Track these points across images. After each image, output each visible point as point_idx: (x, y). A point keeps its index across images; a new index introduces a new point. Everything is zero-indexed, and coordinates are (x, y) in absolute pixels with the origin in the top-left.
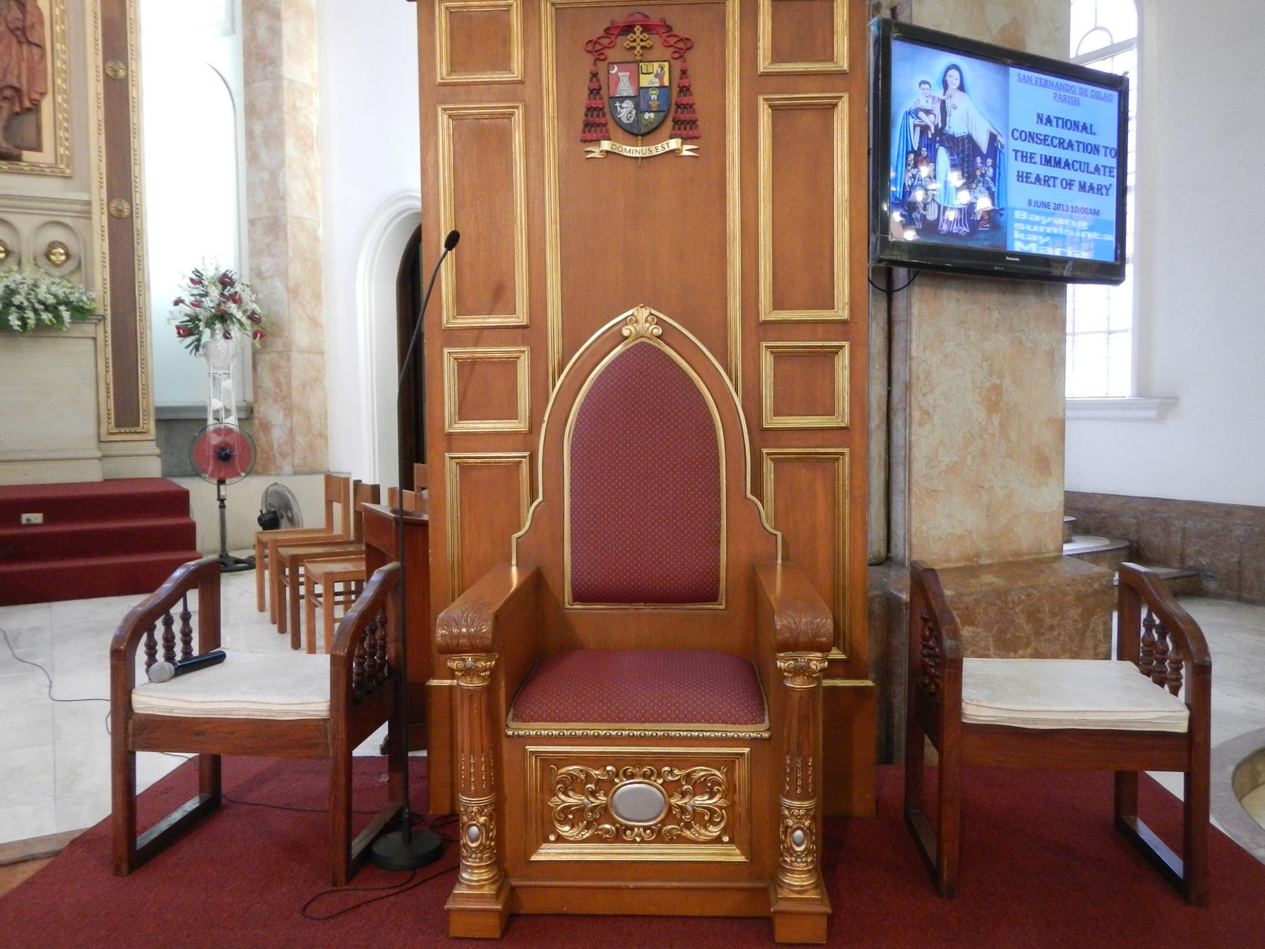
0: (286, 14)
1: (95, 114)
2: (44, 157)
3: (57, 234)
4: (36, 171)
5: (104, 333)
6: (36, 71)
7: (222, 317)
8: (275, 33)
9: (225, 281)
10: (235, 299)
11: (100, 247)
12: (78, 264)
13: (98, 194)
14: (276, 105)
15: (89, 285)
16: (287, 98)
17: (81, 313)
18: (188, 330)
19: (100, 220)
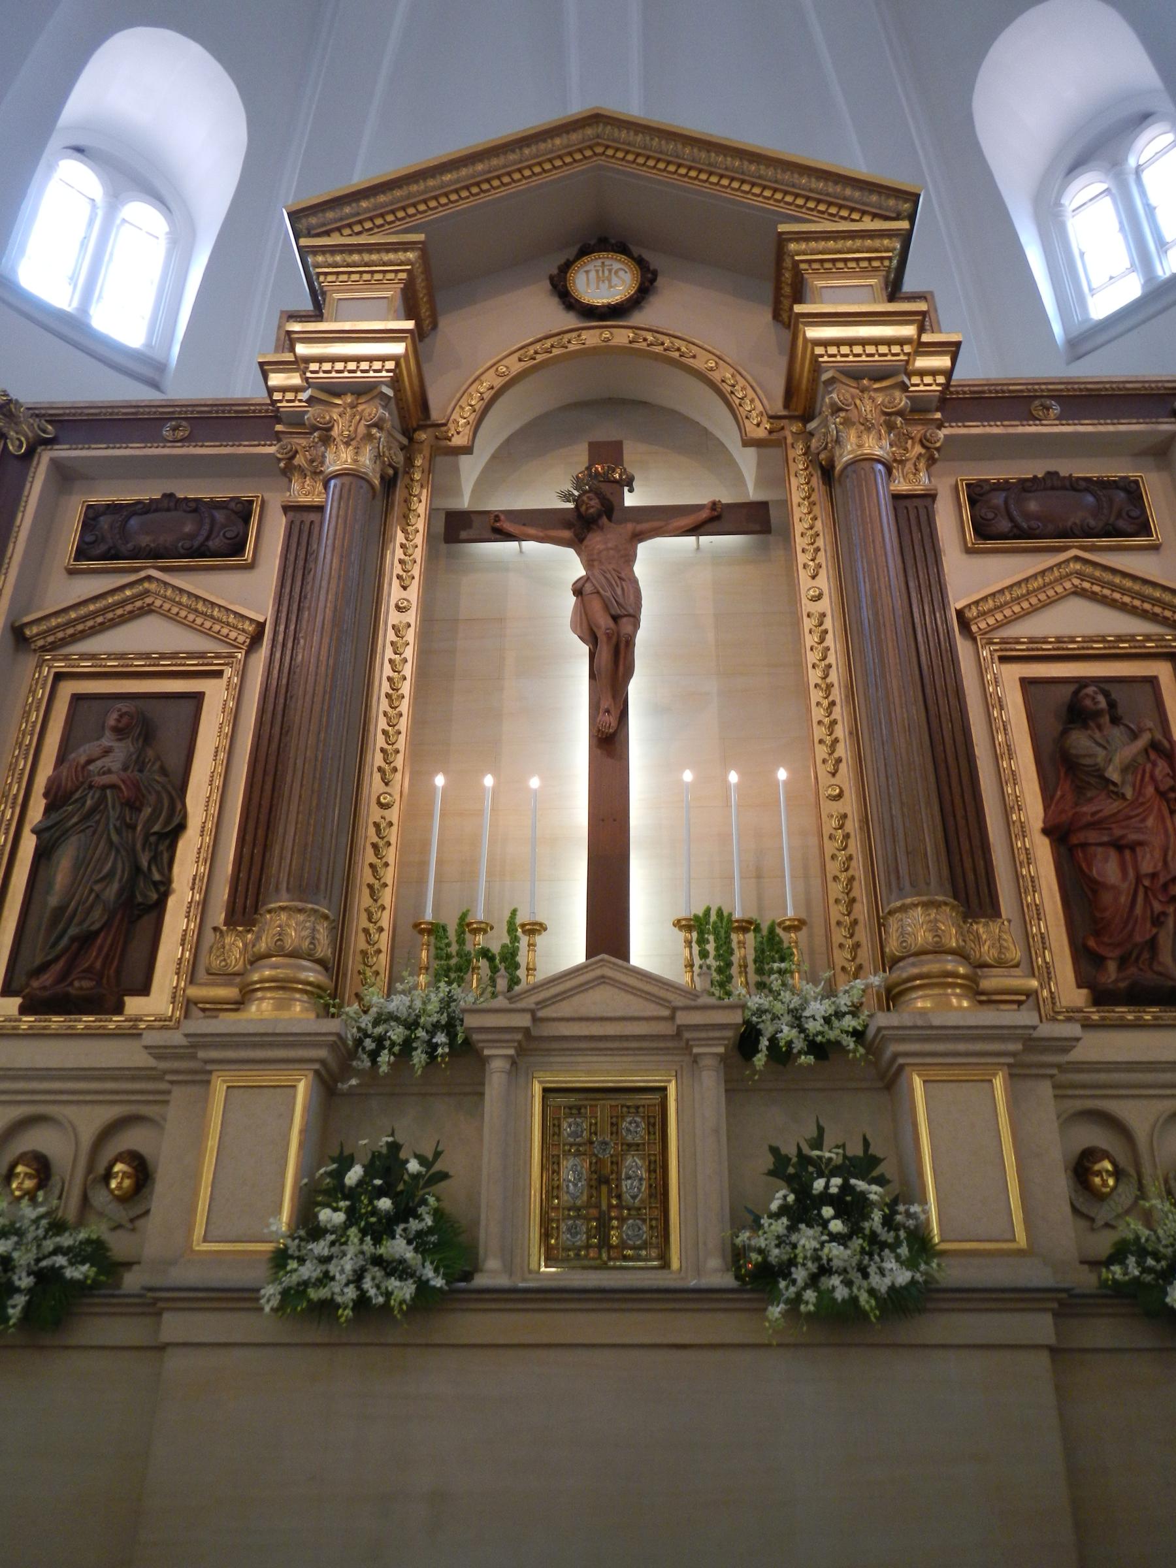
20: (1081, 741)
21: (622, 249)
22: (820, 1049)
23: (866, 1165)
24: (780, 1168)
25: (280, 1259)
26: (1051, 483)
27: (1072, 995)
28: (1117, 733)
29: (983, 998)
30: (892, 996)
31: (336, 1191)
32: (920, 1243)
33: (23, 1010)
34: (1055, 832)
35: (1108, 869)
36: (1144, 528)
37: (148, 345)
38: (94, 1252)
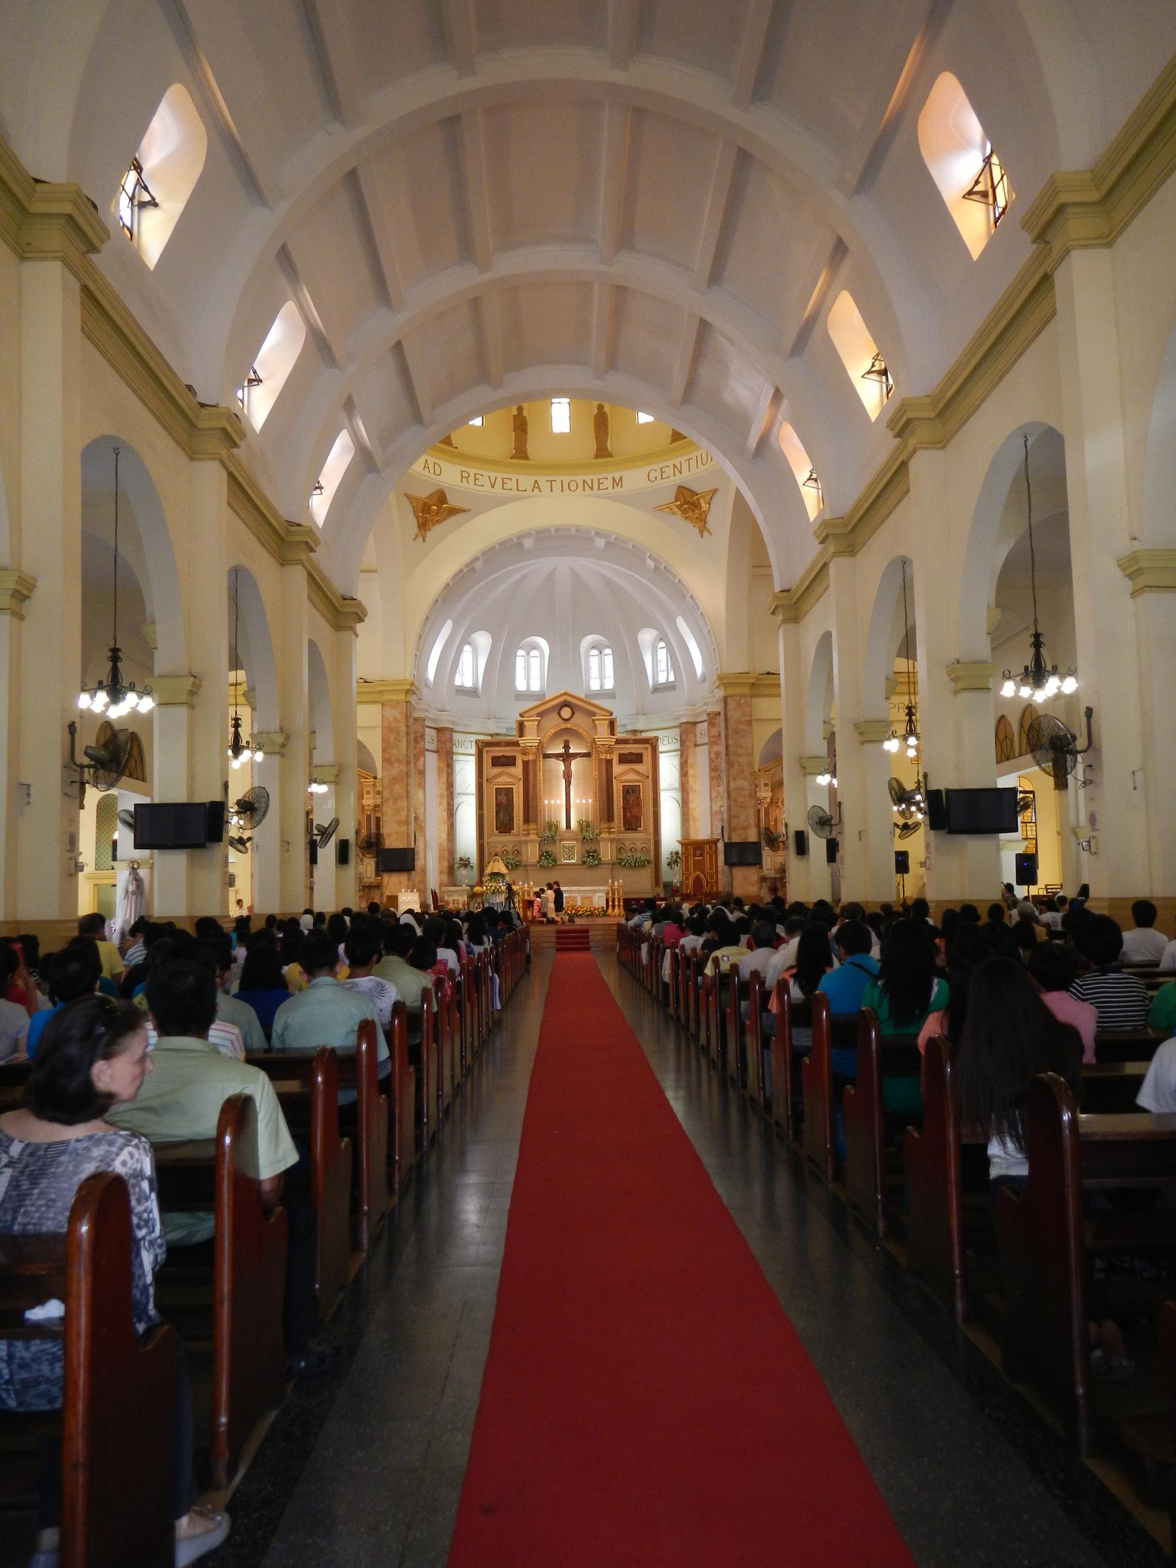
0: (690, 793)
1: (651, 819)
2: (642, 828)
3: (644, 845)
4: (640, 832)
5: (652, 866)
6: (640, 811)
7: (676, 862)
8: (688, 797)
9: (677, 853)
10: (679, 857)
11: (652, 848)
12: (648, 851)
13: (652, 836)
14: (688, 813)
15: (650, 856)
16: (690, 811)
17: (649, 862)
18: (669, 864)
19: (652, 841)
20: (628, 796)
21: (569, 706)
22: (591, 839)
23: (595, 852)
24: (588, 852)
25: (539, 862)
26: (631, 754)
27: (623, 829)
28: (632, 795)
29: (610, 833)
30: (600, 833)
31: (543, 855)
32: (600, 859)
33: (500, 832)
34: (624, 809)
35: (628, 814)
36: (641, 762)
37: (473, 684)
38: (518, 861)
